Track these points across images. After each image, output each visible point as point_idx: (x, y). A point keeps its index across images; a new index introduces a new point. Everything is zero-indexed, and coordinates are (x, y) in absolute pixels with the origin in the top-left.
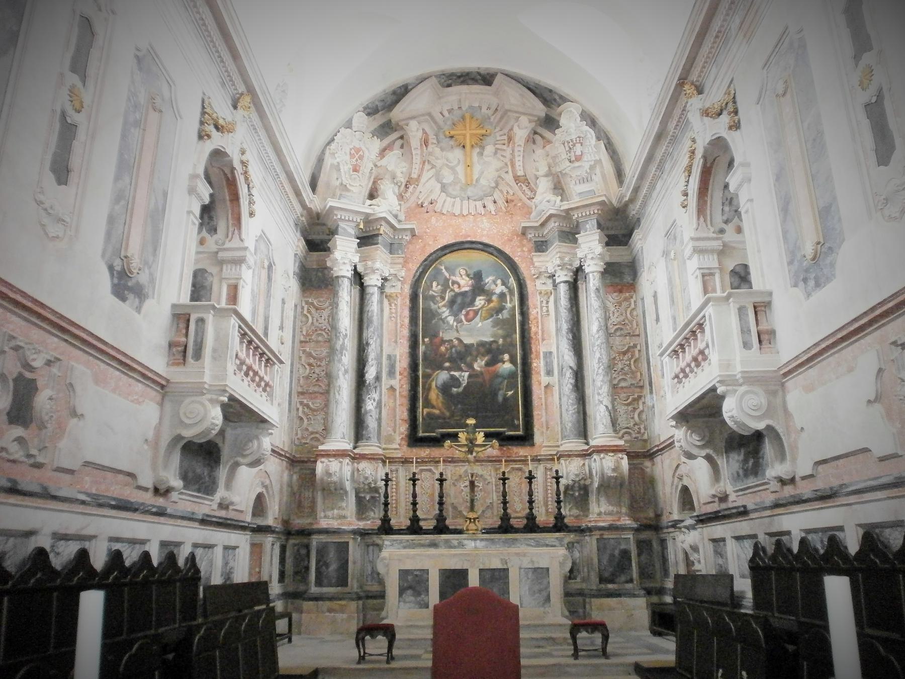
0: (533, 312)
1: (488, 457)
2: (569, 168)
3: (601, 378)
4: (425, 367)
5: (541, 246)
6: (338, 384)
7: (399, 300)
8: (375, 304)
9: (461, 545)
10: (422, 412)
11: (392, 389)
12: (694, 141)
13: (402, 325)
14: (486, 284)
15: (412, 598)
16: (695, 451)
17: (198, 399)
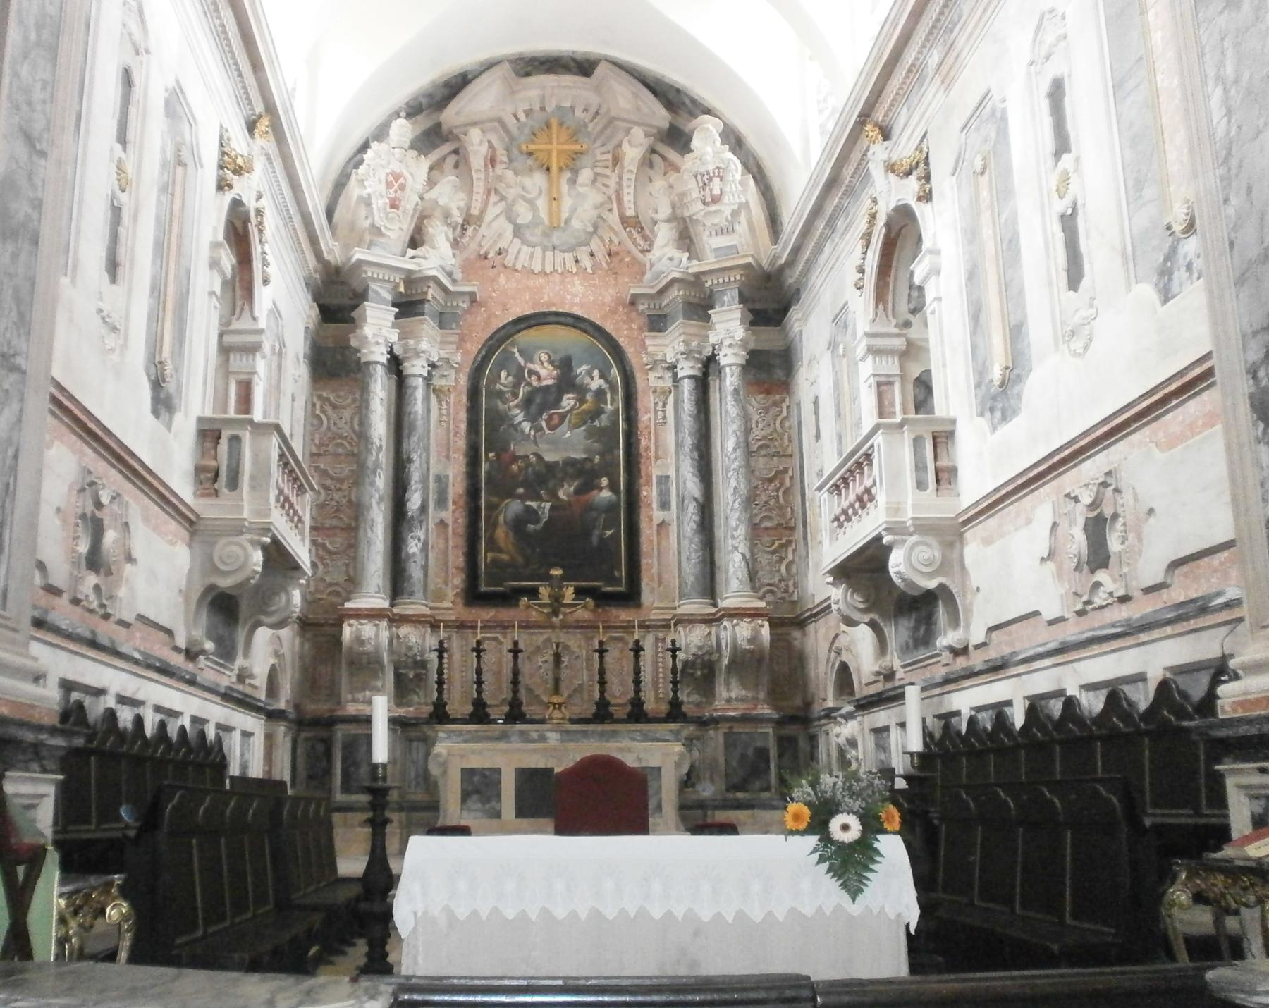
0: (645, 418)
1: (577, 621)
2: (702, 213)
3: (737, 515)
4: (489, 493)
5: (657, 323)
6: (369, 518)
7: (452, 396)
8: (419, 402)
9: (542, 739)
10: (485, 557)
11: (442, 524)
12: (875, 201)
13: (455, 435)
14: (577, 376)
15: (480, 805)
16: (856, 616)
17: (237, 539)
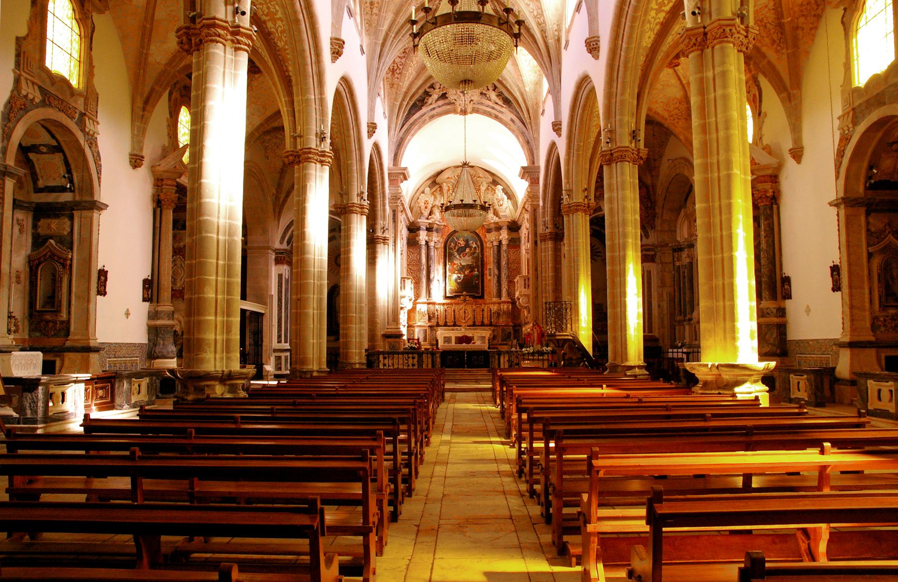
5: (489, 231)
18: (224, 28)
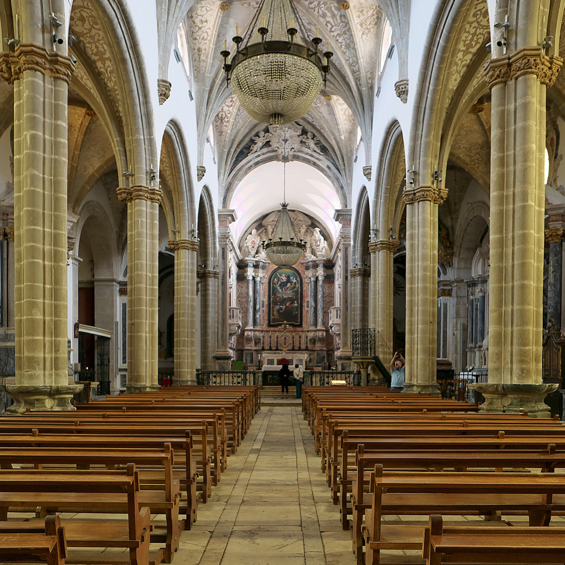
5: (307, 268)
10: (272, 317)
11: (263, 311)
18: (43, 56)
